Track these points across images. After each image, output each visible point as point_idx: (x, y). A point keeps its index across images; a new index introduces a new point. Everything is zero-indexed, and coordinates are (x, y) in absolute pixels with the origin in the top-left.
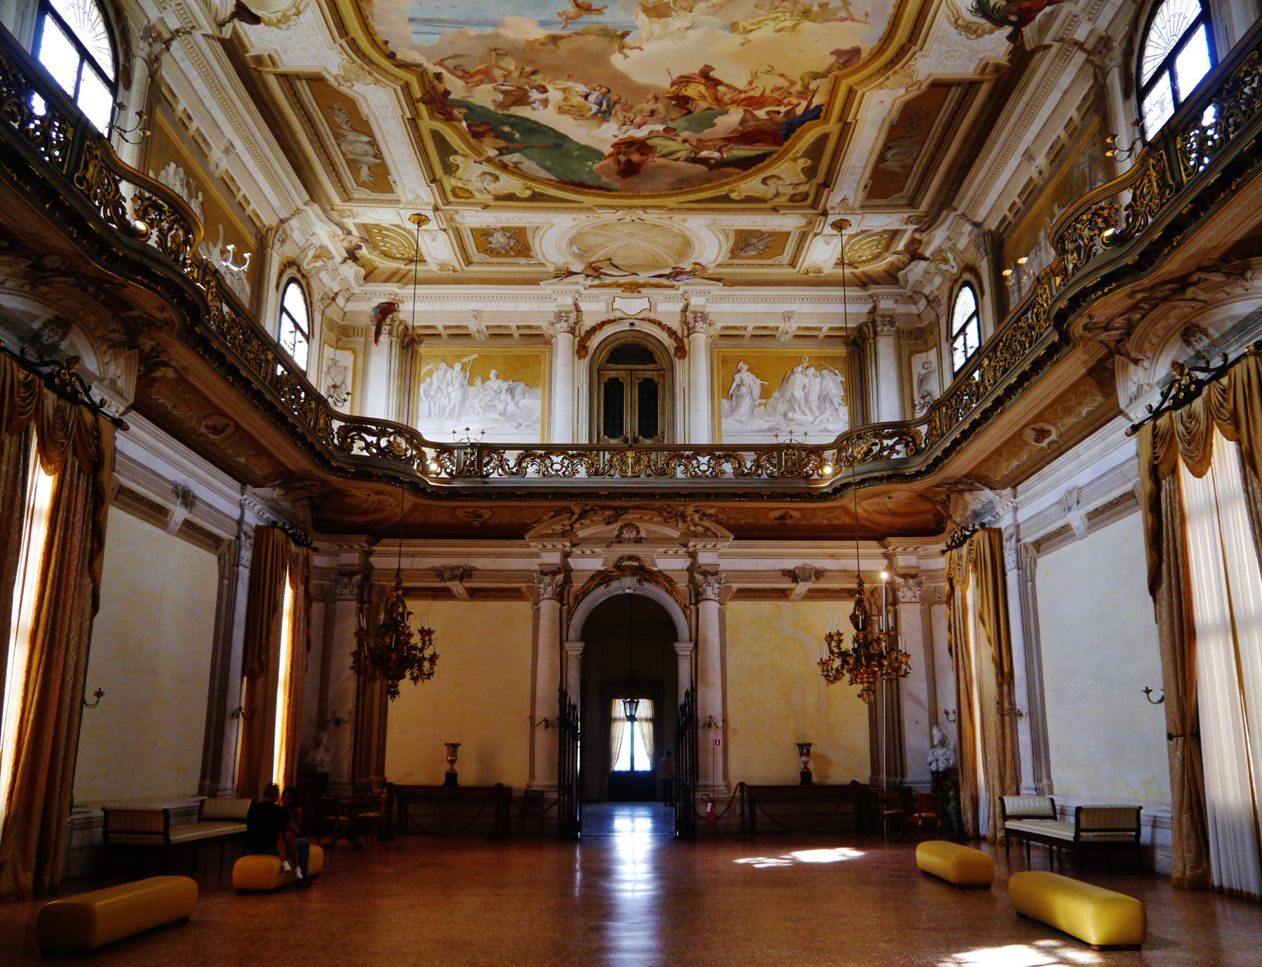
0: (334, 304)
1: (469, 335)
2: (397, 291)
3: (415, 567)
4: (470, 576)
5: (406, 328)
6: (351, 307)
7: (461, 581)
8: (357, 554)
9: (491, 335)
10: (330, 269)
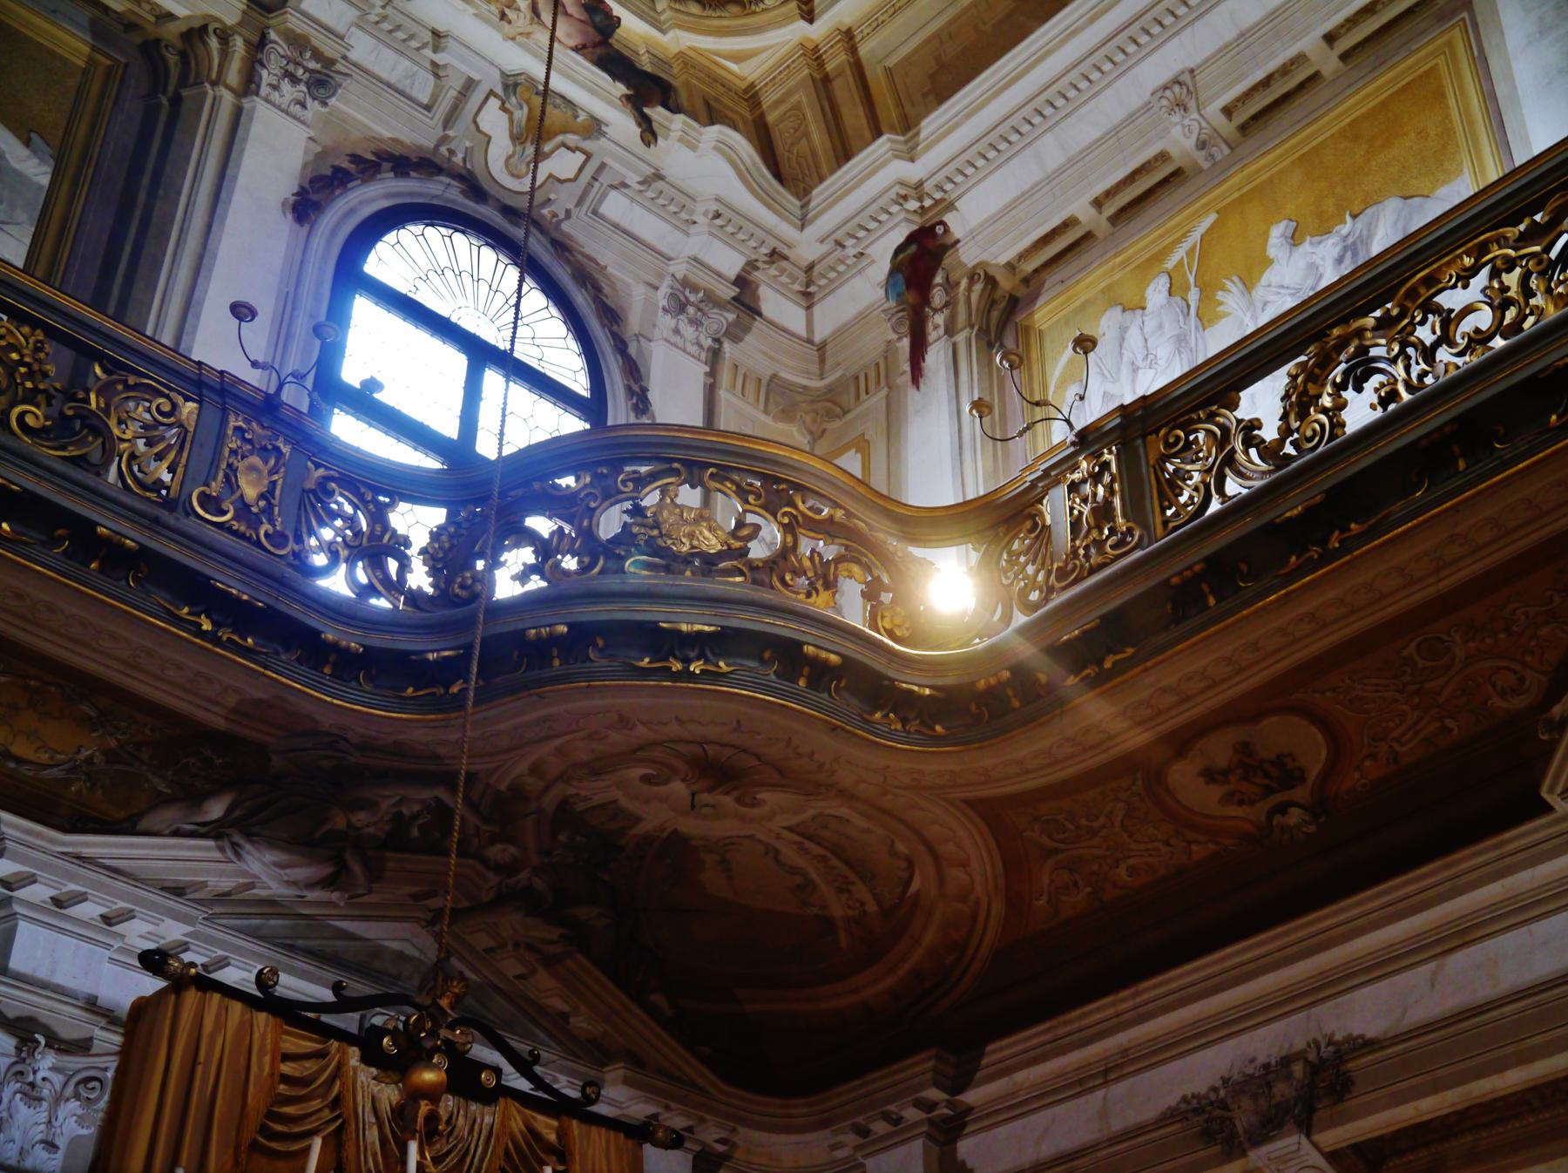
0: (758, 324)
1: (1177, 173)
2: (914, 171)
3: (1117, 1124)
4: (1341, 1088)
5: (991, 281)
6: (831, 315)
7: (1307, 1129)
8: (918, 1145)
9: (1243, 128)
10: (633, 179)
